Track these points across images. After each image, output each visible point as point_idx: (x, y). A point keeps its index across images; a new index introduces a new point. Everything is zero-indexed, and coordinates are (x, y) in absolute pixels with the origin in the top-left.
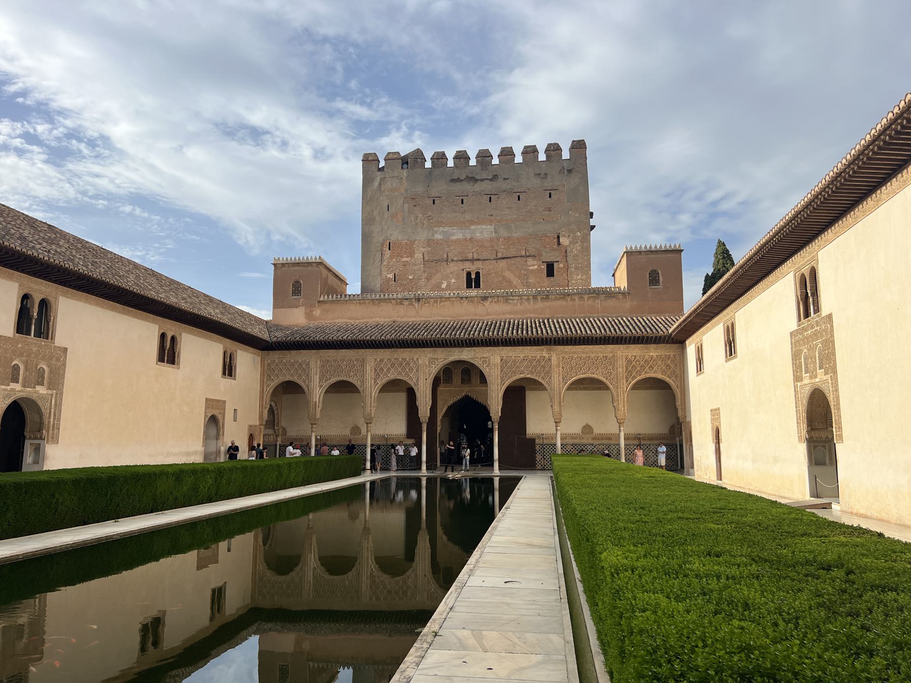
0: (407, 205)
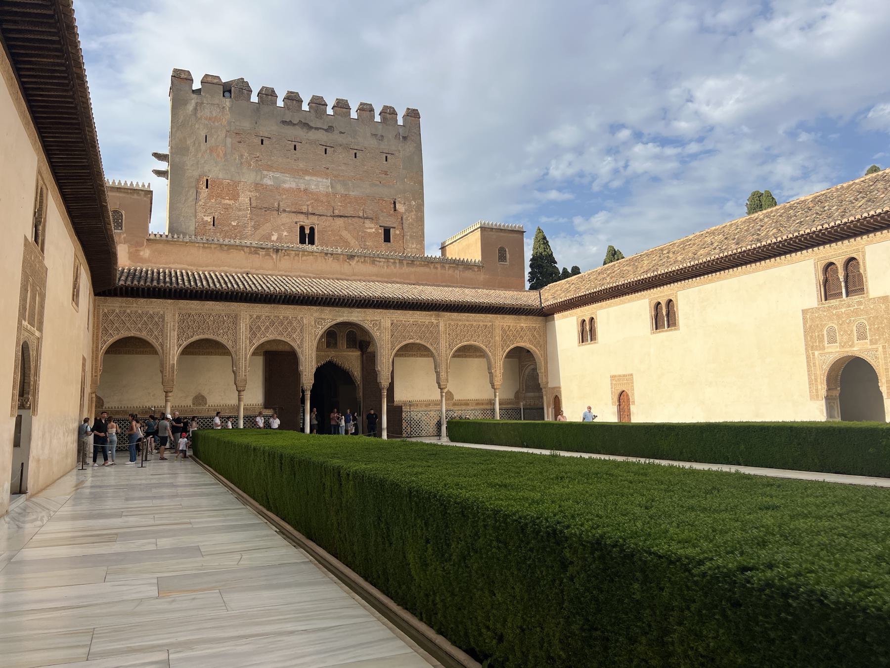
0: (230, 140)
